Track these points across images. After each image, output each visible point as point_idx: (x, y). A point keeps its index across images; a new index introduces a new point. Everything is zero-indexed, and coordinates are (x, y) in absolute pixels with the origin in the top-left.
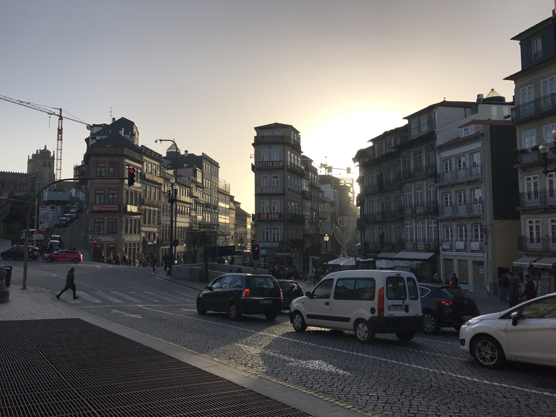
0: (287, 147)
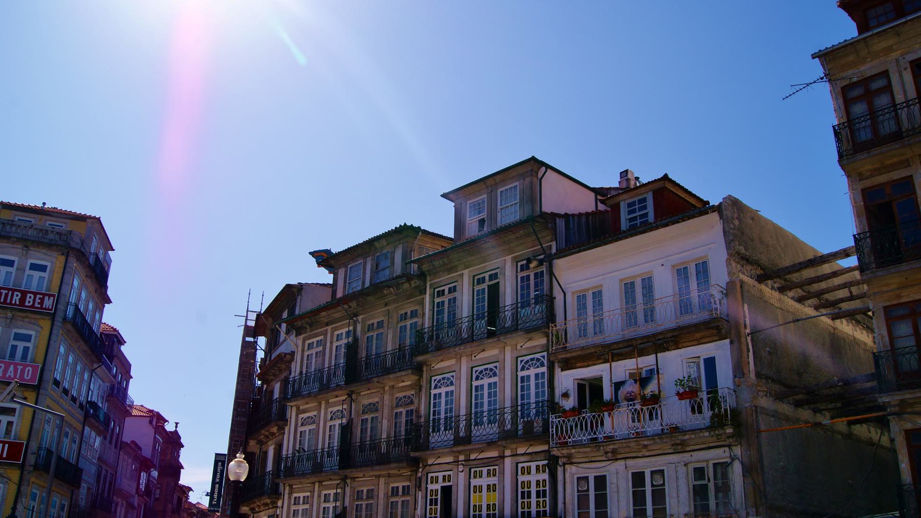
0: (74, 264)
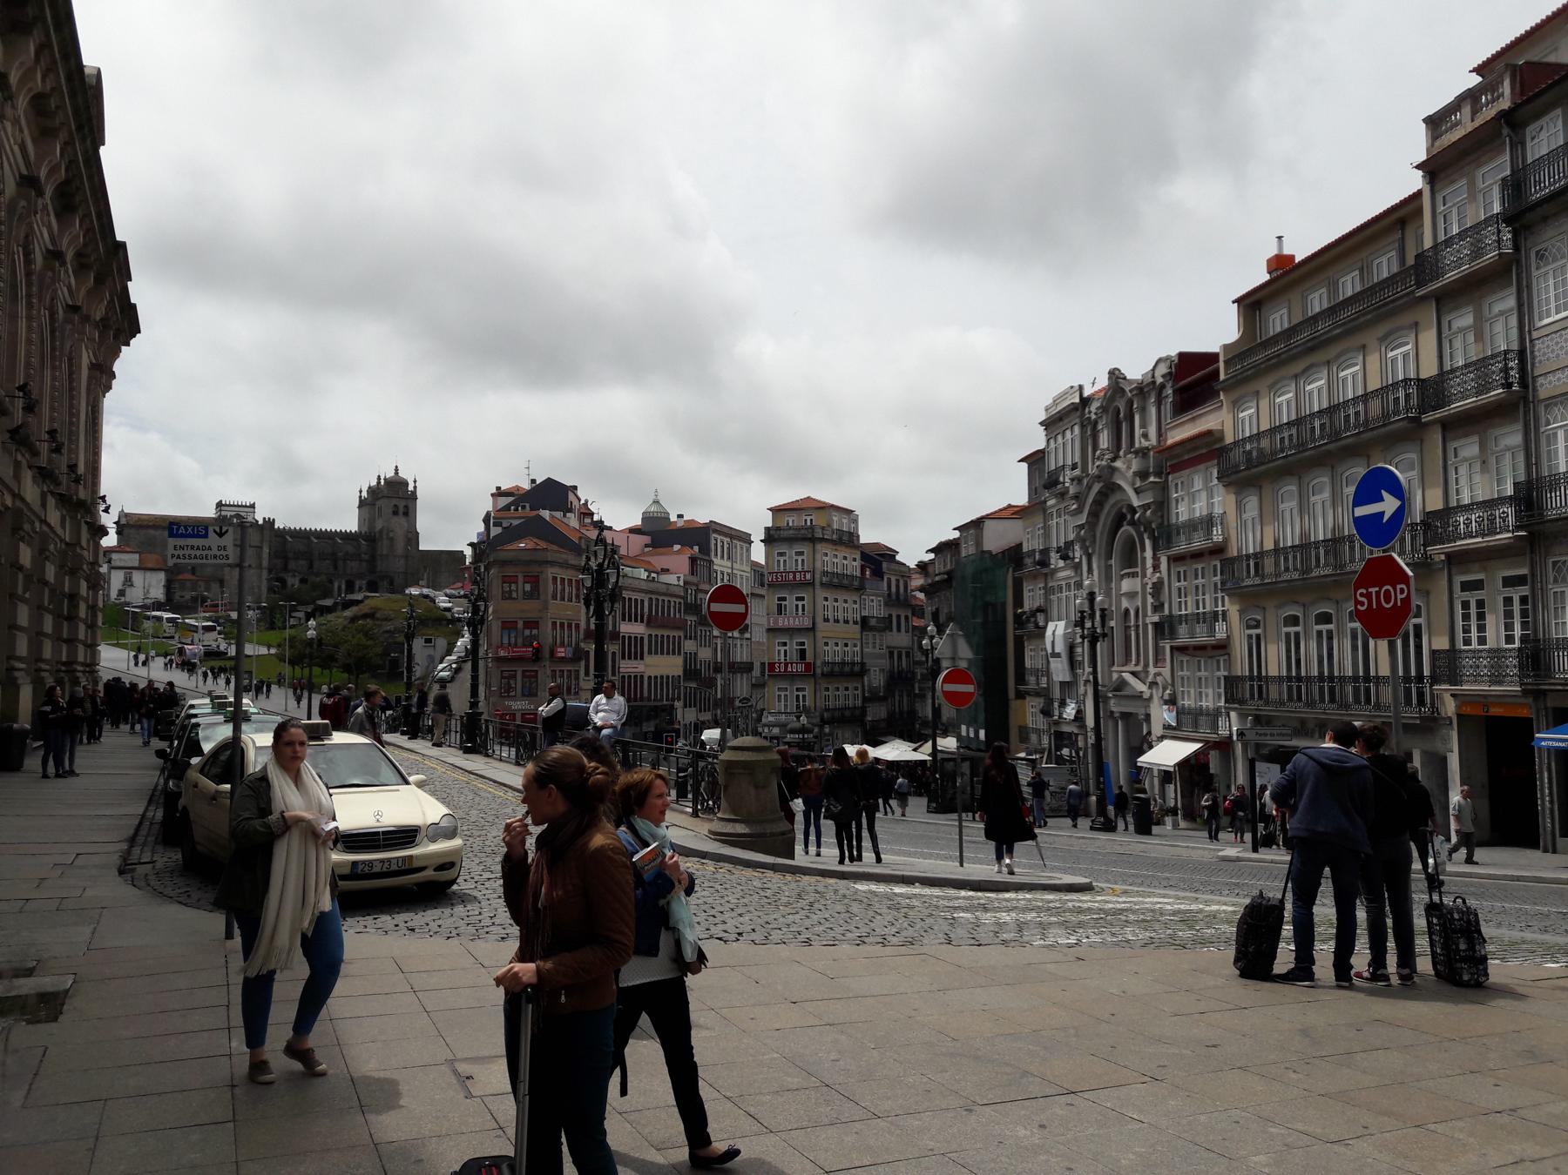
0: (818, 546)
